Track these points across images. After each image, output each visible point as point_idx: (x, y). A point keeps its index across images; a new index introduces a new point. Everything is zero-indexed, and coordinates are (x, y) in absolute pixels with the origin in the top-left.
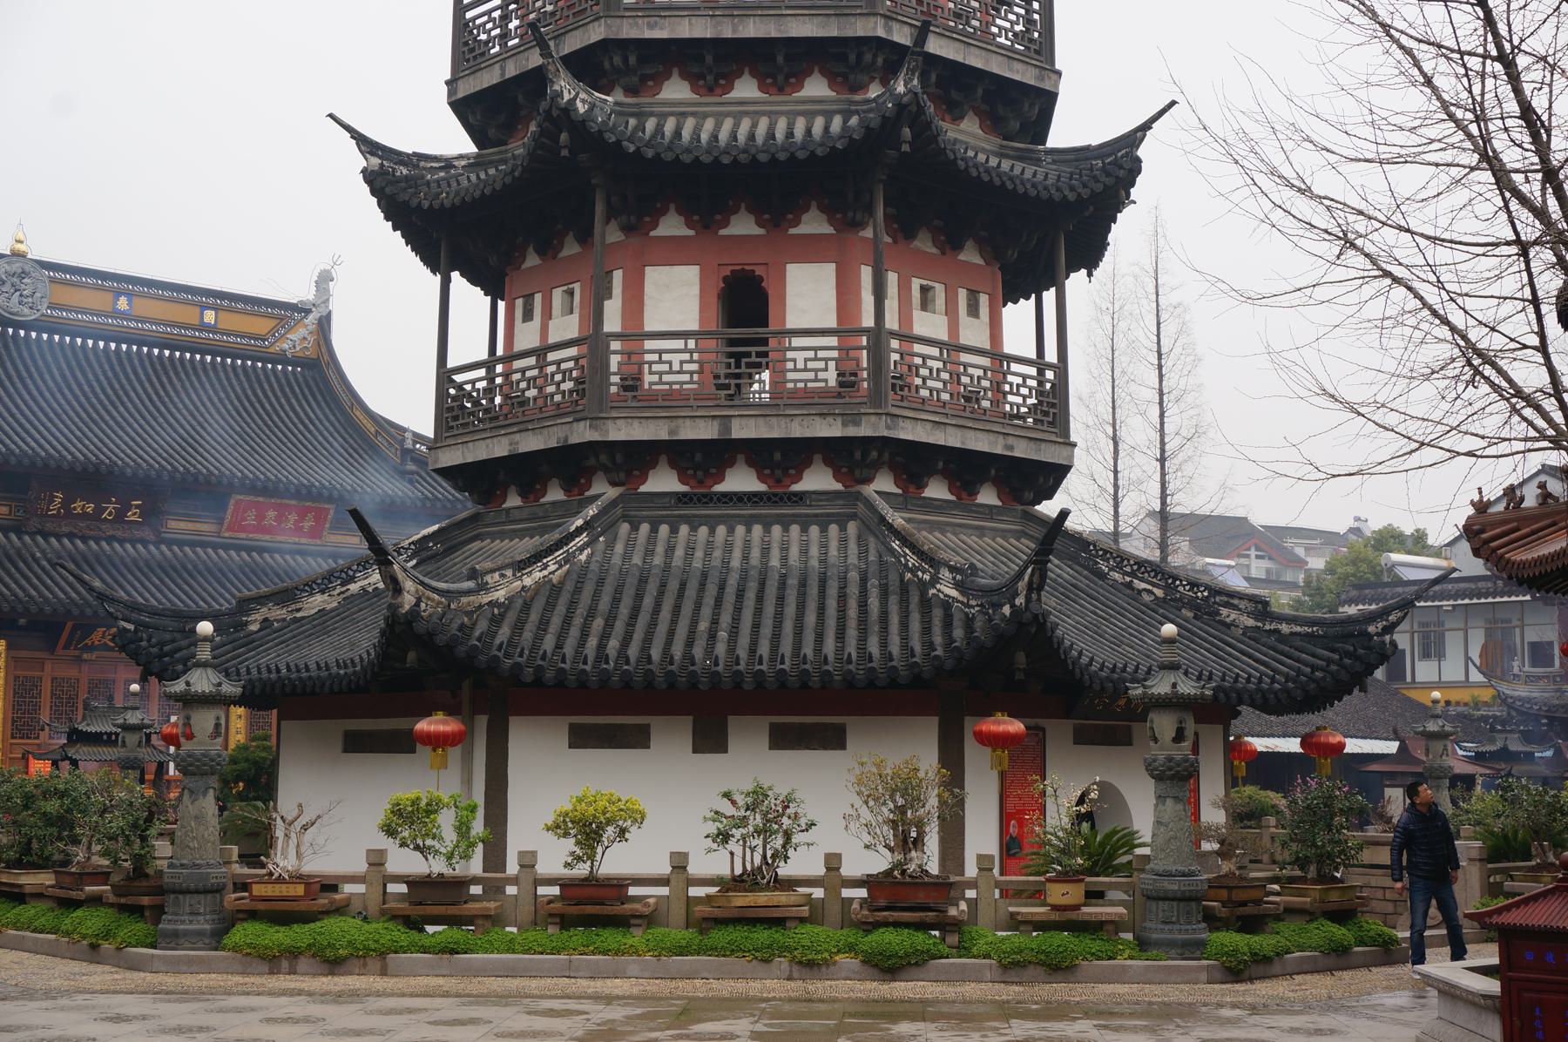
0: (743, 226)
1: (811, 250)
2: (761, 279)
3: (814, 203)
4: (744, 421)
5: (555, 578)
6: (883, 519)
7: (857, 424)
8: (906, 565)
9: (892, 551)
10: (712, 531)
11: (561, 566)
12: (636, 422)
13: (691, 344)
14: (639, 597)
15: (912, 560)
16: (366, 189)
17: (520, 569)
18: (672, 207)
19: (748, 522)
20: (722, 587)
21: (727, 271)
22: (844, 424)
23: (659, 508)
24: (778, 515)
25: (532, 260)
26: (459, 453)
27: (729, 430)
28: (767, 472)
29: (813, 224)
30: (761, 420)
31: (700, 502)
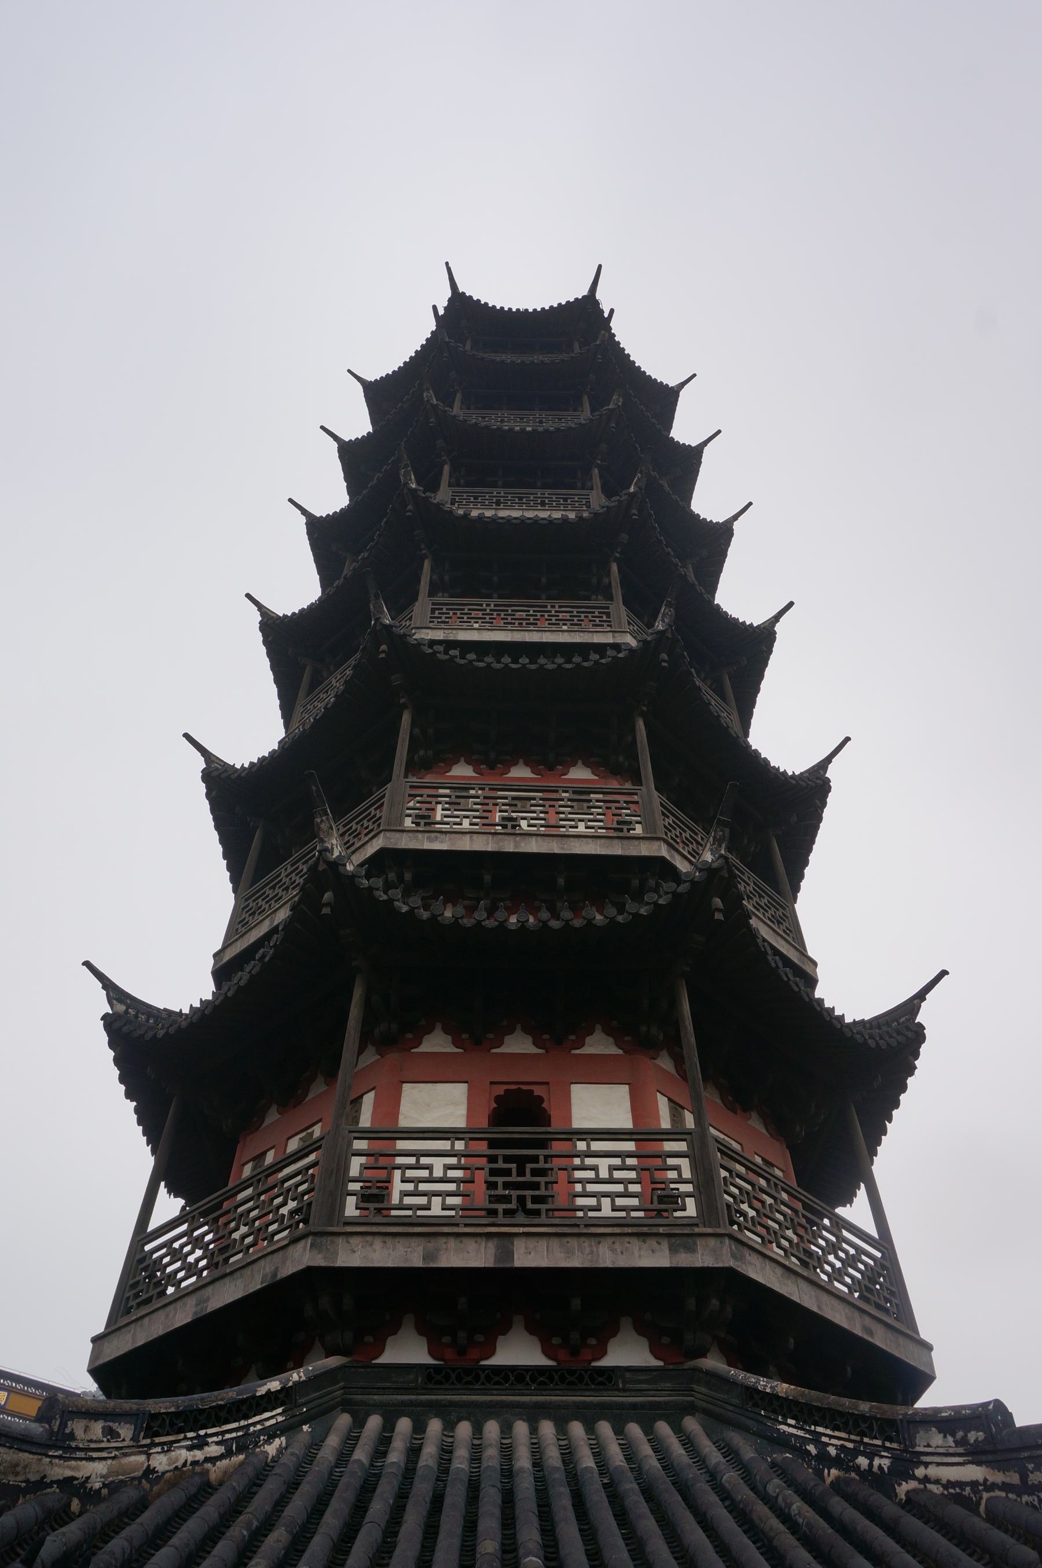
0: (519, 1045)
1: (598, 1073)
2: (541, 1099)
3: (598, 1027)
4: (531, 1243)
5: (215, 1472)
6: (752, 1392)
7: (691, 1249)
8: (823, 1457)
9: (783, 1442)
10: (478, 1430)
11: (228, 1454)
12: (378, 1242)
13: (460, 1145)
14: (360, 1507)
15: (834, 1441)
16: (104, 1038)
17: (151, 1433)
18: (439, 1026)
19: (533, 1415)
20: (508, 1498)
21: (500, 1090)
22: (673, 1250)
23: (398, 1390)
24: (577, 1406)
25: (272, 1116)
26: (129, 1337)
27: (510, 1255)
28: (556, 1341)
29: (598, 1045)
30: (555, 1242)
31: (460, 1379)
